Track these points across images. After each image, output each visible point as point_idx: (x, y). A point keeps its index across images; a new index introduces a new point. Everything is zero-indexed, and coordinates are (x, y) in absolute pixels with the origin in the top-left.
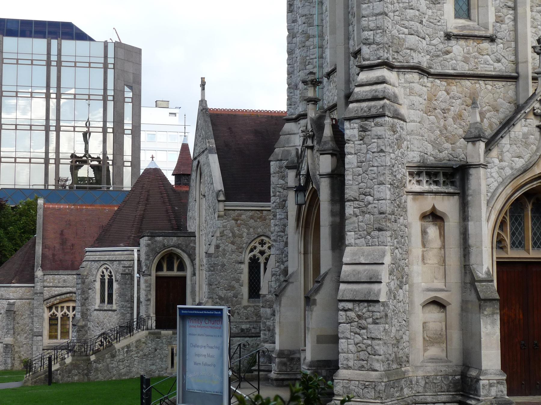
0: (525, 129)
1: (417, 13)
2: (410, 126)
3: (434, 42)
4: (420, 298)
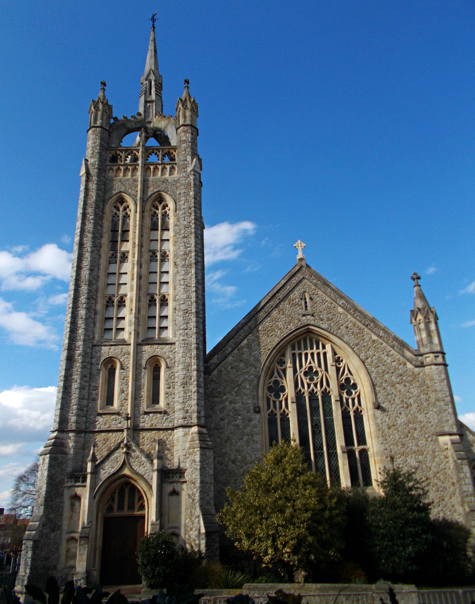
3: (91, 417)
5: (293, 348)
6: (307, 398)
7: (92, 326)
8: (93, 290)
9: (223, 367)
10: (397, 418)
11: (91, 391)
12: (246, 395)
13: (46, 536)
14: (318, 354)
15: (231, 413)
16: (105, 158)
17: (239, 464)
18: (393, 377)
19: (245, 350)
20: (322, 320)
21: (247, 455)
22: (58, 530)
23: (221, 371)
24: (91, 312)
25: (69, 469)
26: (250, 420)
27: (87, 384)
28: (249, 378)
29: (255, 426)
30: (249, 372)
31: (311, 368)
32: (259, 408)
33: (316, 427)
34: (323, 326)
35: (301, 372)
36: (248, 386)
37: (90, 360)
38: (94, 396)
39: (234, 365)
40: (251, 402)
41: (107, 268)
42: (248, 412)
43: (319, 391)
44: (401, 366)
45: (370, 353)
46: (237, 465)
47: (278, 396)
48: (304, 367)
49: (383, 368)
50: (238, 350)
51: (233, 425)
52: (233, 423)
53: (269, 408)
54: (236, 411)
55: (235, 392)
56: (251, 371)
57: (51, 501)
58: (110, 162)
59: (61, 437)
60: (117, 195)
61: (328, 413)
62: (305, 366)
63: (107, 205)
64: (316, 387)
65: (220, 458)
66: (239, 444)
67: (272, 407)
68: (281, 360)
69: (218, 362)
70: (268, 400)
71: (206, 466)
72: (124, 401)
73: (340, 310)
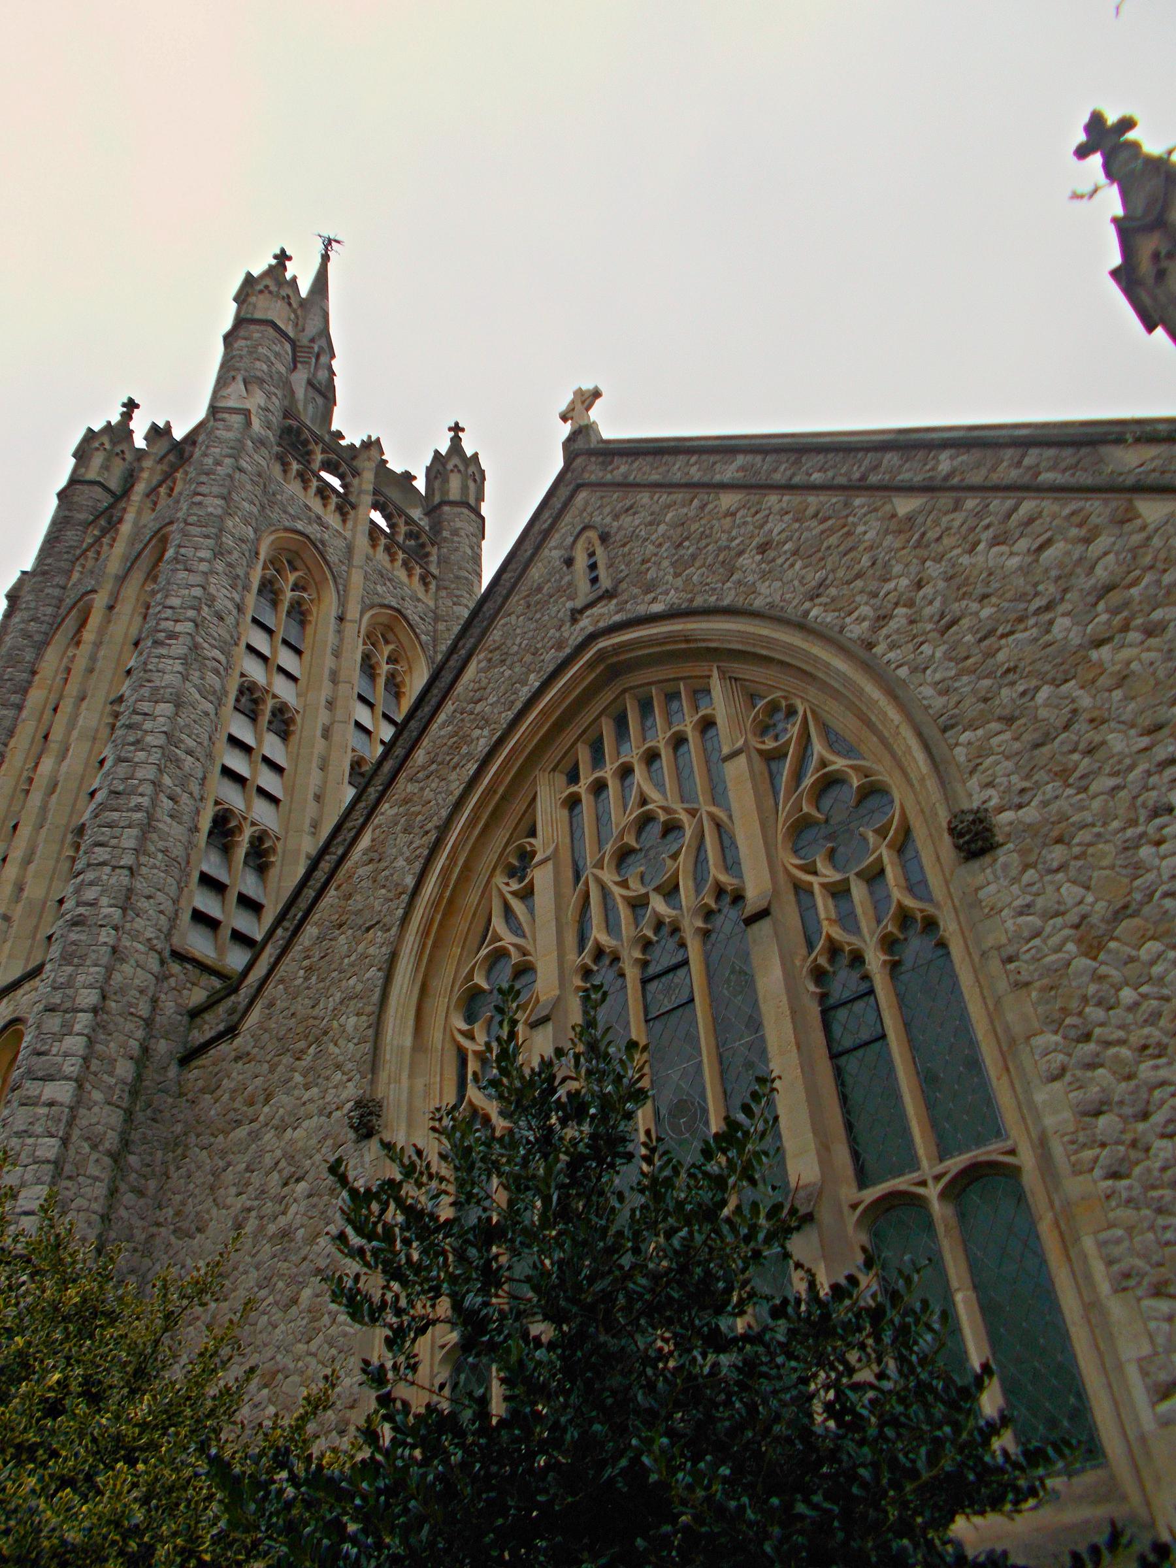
10: (1145, 852)
12: (338, 1067)
18: (1062, 623)
49: (986, 613)
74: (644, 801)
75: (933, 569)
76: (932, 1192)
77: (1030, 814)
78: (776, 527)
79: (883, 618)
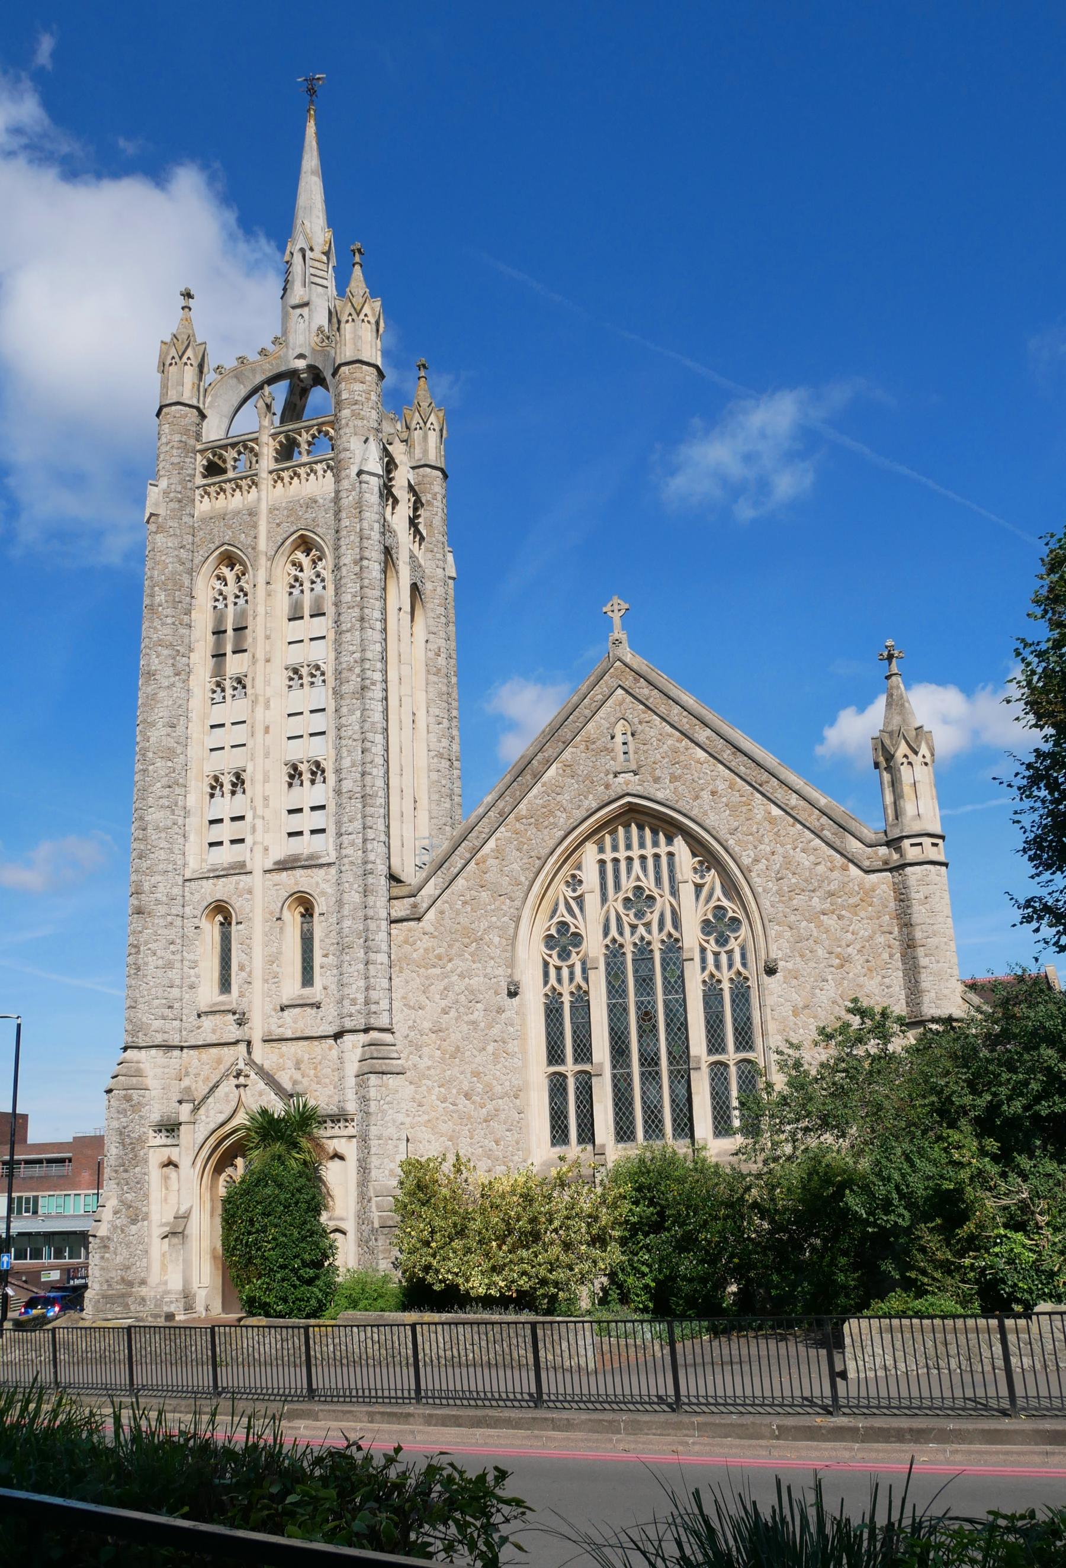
0: (227, 1089)
1: (164, 1001)
2: (153, 1093)
4: (157, 1231)
5: (601, 850)
6: (629, 957)
7: (181, 840)
8: (179, 767)
9: (447, 902)
11: (186, 969)
12: (492, 958)
13: (122, 1231)
14: (657, 856)
15: (462, 998)
16: (190, 472)
17: (477, 1099)
18: (816, 900)
19: (491, 862)
20: (657, 780)
21: (495, 1083)
22: (143, 1220)
23: (442, 913)
24: (176, 812)
25: (155, 1117)
26: (500, 1010)
27: (178, 957)
28: (499, 924)
29: (509, 1023)
30: (499, 909)
31: (638, 889)
32: (517, 985)
33: (646, 1017)
34: (660, 796)
35: (616, 900)
36: (496, 940)
37: (180, 909)
38: (193, 979)
39: (468, 897)
40: (502, 973)
41: (205, 716)
42: (497, 993)
43: (656, 939)
44: (836, 874)
45: (766, 848)
46: (473, 1103)
47: (564, 955)
48: (624, 889)
49: (794, 881)
50: (477, 864)
51: (468, 1023)
52: (466, 1018)
53: (546, 983)
54: (472, 992)
55: (472, 955)
56: (503, 907)
57: (126, 1171)
58: (205, 477)
59: (135, 1059)
60: (217, 552)
61: (673, 987)
62: (628, 885)
63: (200, 577)
64: (649, 932)
65: (442, 1089)
66: (478, 1060)
67: (553, 980)
68: (574, 876)
69: (438, 892)
70: (546, 964)
71: (386, 1107)
72: (246, 986)
73: (701, 754)
74: (638, 879)
75: (780, 850)
76: (731, 1063)
77: (790, 965)
78: (721, 786)
79: (756, 861)
